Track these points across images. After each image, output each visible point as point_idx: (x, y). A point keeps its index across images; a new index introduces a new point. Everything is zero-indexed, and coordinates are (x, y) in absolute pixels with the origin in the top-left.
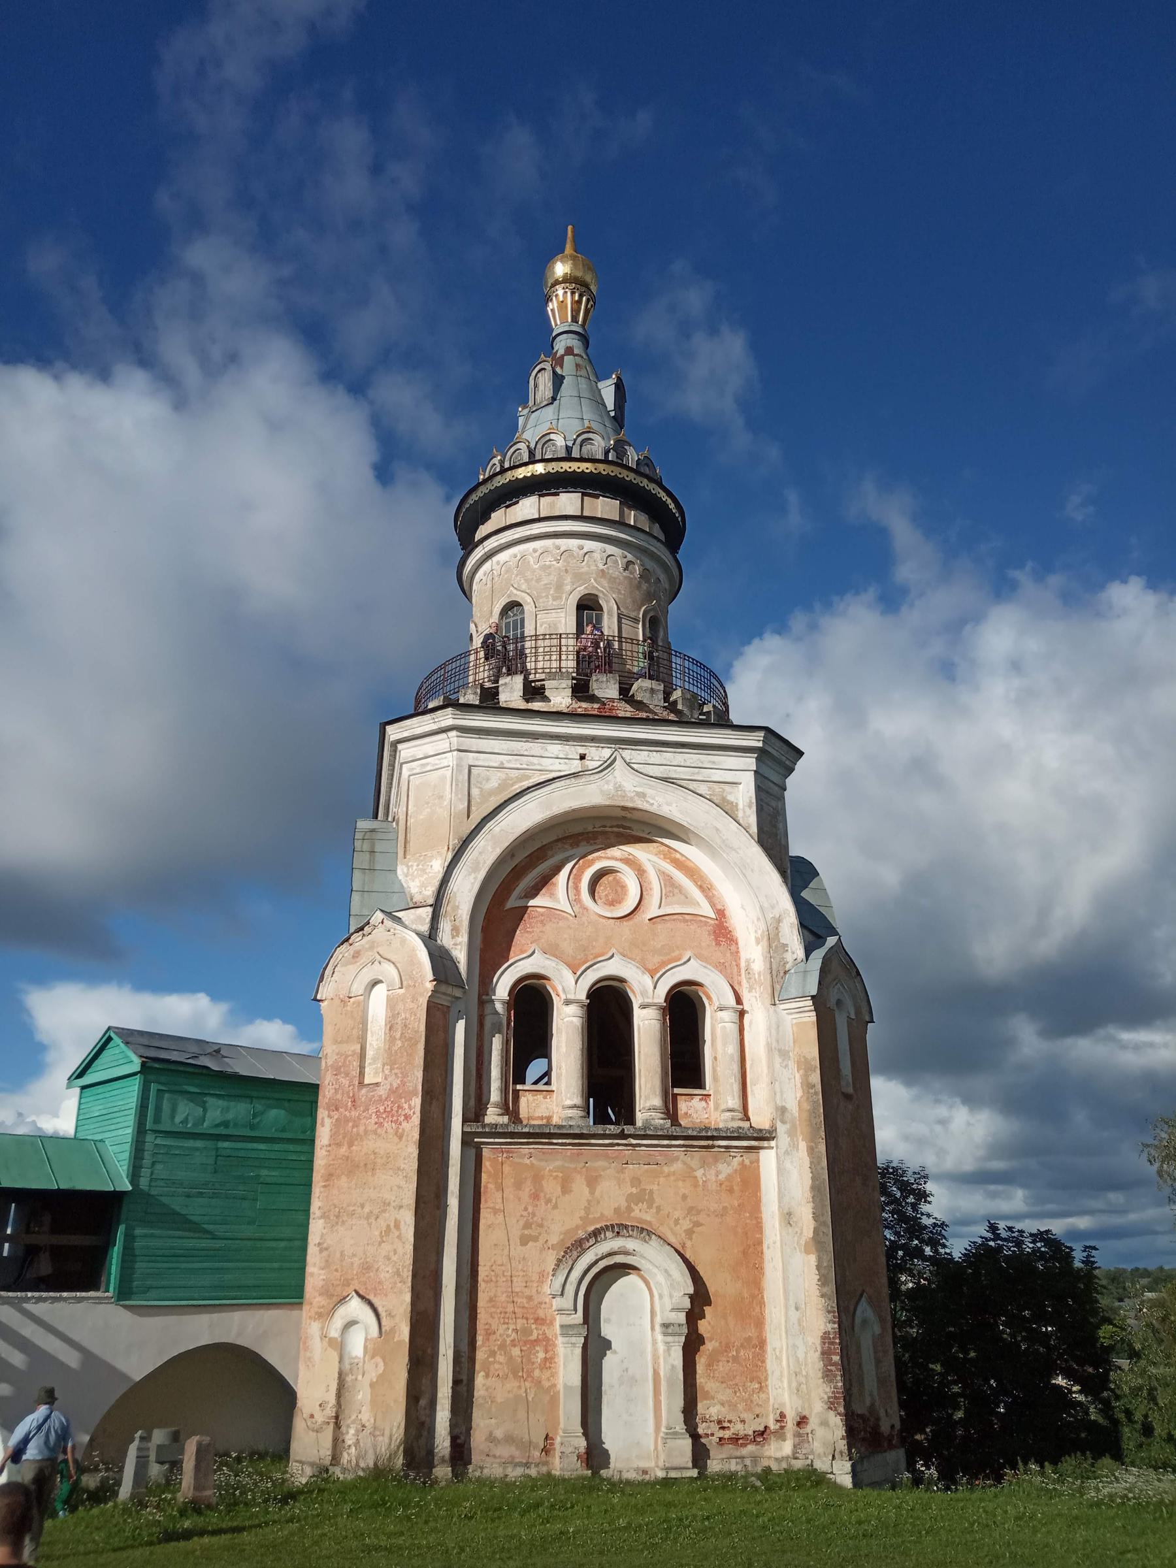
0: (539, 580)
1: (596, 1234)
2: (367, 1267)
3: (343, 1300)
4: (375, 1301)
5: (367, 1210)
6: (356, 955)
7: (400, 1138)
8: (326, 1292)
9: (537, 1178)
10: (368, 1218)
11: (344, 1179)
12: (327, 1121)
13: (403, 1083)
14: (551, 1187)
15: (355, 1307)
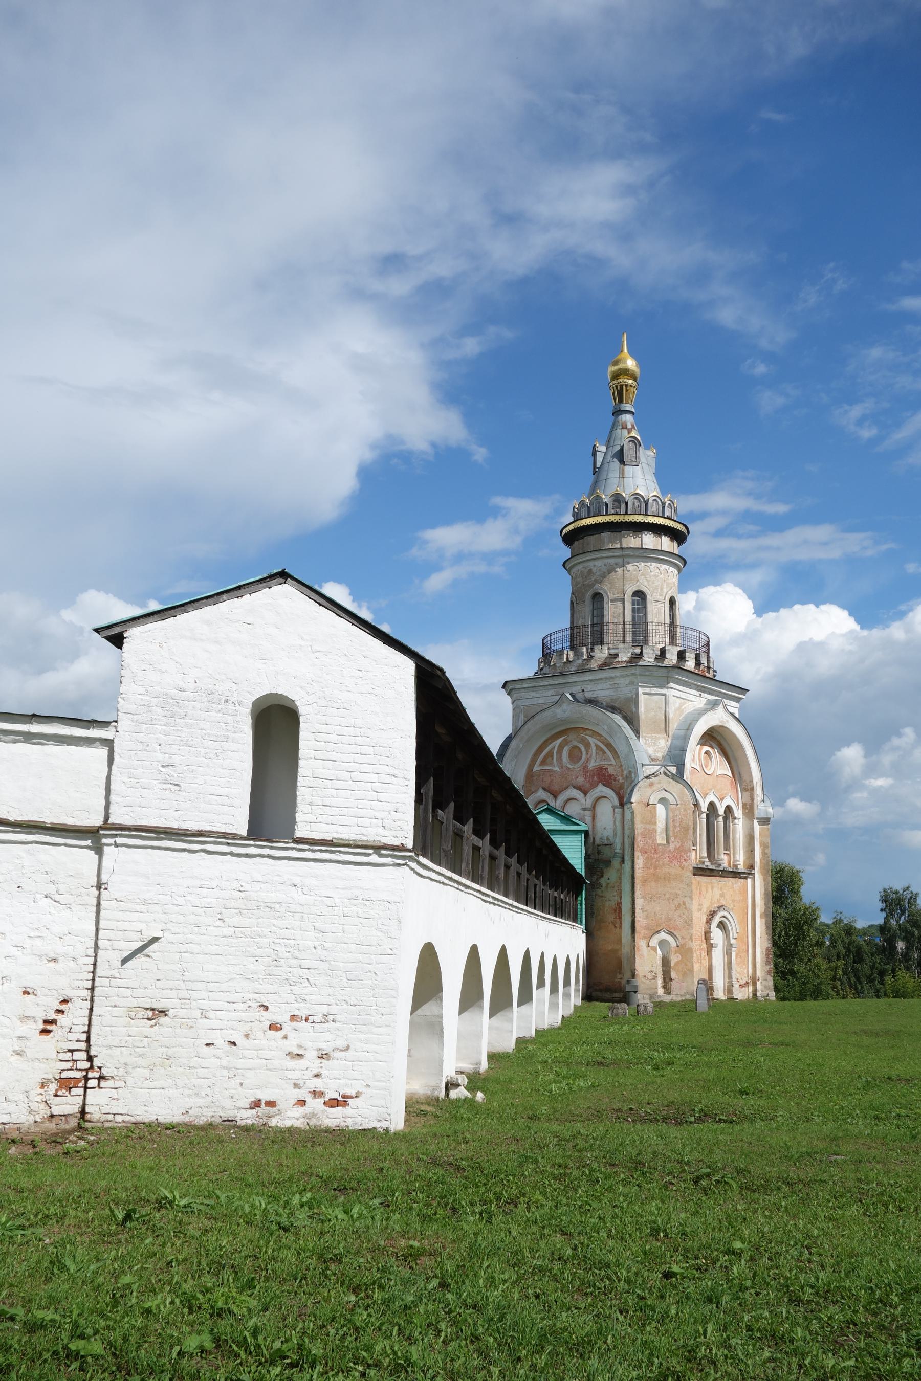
0: (653, 582)
1: (719, 908)
2: (669, 919)
3: (658, 932)
4: (675, 933)
5: (667, 896)
6: (651, 785)
7: (683, 868)
8: (647, 928)
9: (700, 887)
10: (668, 900)
11: (653, 884)
12: (641, 857)
13: (682, 846)
14: (704, 890)
15: (663, 936)
